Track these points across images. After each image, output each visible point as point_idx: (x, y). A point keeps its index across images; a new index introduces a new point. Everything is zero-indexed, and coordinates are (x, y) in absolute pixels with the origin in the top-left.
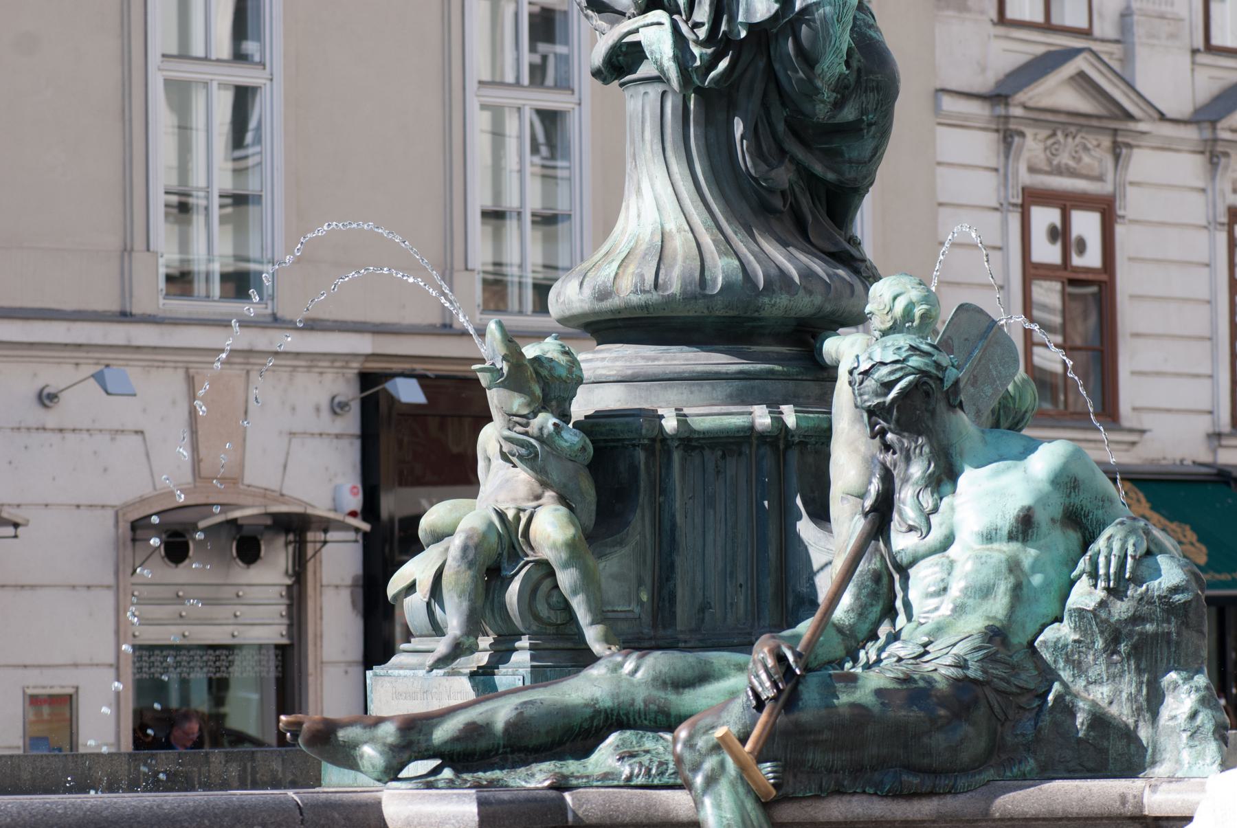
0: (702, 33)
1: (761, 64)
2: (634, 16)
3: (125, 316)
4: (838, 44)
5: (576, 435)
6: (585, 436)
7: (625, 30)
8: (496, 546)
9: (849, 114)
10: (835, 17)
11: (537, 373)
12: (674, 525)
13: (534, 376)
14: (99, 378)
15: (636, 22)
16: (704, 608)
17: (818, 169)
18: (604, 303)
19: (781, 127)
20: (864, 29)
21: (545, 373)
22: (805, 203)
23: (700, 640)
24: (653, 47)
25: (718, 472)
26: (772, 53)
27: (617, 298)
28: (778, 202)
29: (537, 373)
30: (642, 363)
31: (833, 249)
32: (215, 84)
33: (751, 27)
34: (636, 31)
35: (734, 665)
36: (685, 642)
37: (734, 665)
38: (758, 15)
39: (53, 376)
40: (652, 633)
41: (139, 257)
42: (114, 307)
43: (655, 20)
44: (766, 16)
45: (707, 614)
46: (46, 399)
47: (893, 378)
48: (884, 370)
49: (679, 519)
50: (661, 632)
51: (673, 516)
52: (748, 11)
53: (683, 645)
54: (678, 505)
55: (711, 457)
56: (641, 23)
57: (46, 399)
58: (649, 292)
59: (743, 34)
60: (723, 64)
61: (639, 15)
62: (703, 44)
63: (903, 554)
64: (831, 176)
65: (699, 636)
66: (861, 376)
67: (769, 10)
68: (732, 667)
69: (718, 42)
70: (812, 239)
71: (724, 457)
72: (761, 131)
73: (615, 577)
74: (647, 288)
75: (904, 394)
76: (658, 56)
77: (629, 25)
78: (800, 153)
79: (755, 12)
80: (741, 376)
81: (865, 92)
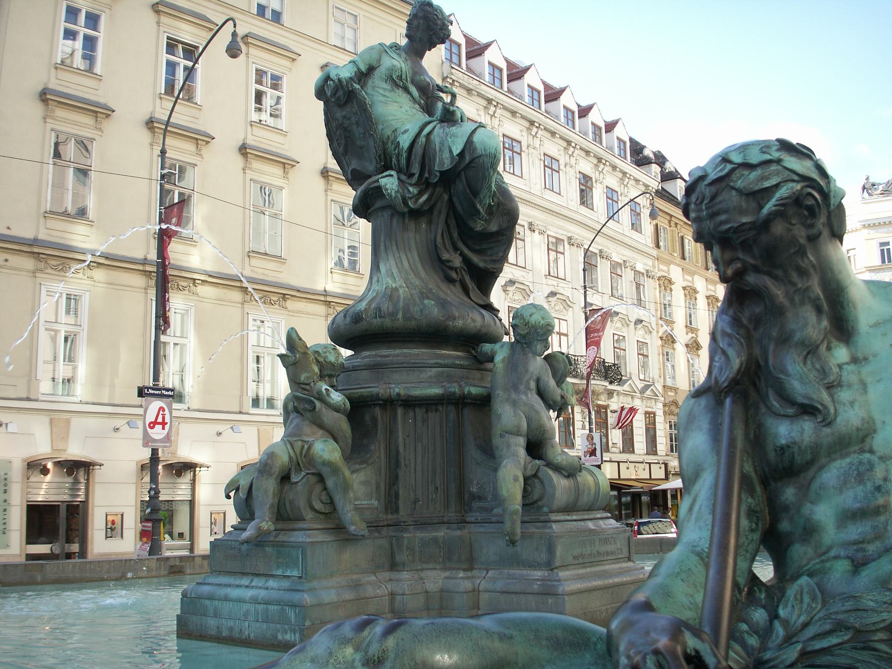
0: (414, 180)
1: (446, 197)
3: (241, 413)
4: (489, 183)
5: (339, 396)
6: (345, 398)
8: (287, 464)
9: (493, 228)
10: (489, 165)
11: (317, 360)
12: (398, 452)
13: (315, 361)
14: (232, 428)
16: (415, 502)
17: (475, 259)
18: (358, 325)
19: (455, 235)
20: (500, 183)
21: (321, 359)
22: (467, 279)
23: (414, 521)
25: (424, 421)
26: (452, 191)
27: (365, 321)
28: (454, 275)
29: (317, 360)
30: (379, 359)
31: (482, 303)
32: (266, 353)
33: (442, 172)
35: (547, 639)
36: (405, 522)
37: (547, 639)
39: (220, 427)
40: (385, 517)
41: (245, 397)
42: (238, 410)
45: (417, 505)
46: (219, 434)
47: (767, 184)
48: (754, 175)
49: (401, 449)
50: (390, 516)
51: (398, 447)
52: (442, 163)
53: (404, 524)
54: (400, 439)
55: (419, 412)
57: (219, 434)
58: (384, 317)
60: (425, 197)
63: (796, 450)
64: (481, 265)
65: (412, 519)
66: (713, 189)
68: (544, 642)
69: (424, 184)
70: (473, 299)
71: (427, 411)
72: (445, 236)
73: (362, 483)
74: (383, 315)
75: (784, 204)
76: (389, 191)
78: (466, 251)
79: (444, 164)
80: (437, 366)
81: (502, 216)
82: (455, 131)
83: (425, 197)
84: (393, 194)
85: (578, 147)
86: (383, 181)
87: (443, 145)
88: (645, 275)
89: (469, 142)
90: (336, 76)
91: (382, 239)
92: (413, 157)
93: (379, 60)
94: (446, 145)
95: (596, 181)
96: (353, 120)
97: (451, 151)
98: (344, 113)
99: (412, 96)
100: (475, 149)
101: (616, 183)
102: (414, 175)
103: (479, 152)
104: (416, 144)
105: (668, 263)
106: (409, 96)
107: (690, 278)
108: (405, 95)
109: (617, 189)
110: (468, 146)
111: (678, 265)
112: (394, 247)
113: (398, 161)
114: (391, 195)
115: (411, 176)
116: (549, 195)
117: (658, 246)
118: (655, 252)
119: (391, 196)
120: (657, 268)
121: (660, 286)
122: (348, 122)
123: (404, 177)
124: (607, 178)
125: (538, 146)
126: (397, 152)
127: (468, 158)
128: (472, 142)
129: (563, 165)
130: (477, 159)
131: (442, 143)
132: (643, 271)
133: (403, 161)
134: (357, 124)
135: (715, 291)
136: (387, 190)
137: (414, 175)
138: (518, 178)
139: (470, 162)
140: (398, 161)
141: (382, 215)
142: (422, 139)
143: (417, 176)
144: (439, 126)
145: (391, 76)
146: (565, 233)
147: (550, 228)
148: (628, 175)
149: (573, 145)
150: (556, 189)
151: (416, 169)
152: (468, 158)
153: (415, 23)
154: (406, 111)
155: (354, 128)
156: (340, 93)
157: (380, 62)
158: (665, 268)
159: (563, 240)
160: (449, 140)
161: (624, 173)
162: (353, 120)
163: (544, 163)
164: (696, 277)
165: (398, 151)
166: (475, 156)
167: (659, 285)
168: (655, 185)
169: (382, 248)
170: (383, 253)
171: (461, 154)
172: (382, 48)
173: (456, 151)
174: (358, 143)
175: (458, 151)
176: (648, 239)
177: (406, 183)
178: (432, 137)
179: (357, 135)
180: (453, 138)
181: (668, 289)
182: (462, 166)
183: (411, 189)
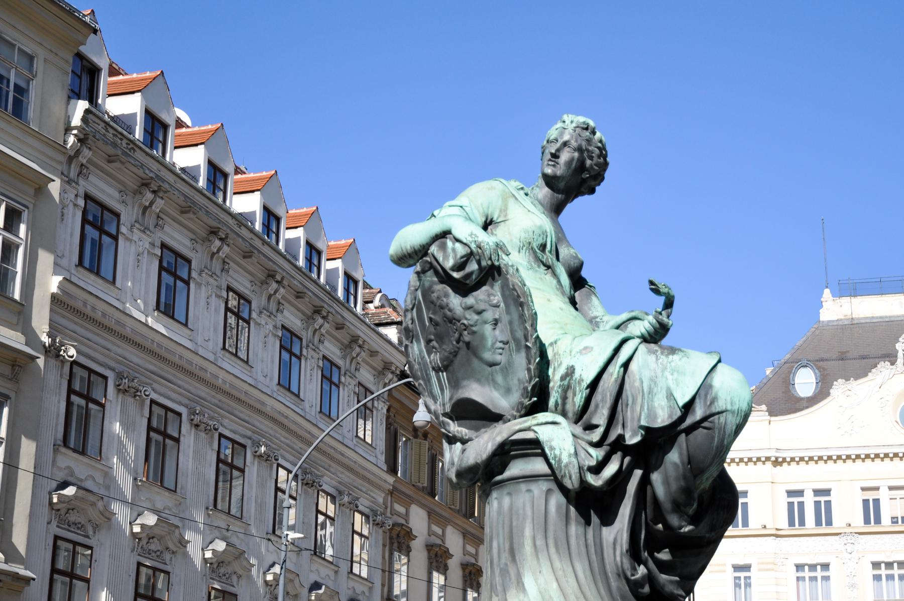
0: (596, 436)
1: (638, 473)
2: (515, 418)
7: (517, 428)
15: (525, 422)
24: (554, 444)
33: (648, 430)
34: (528, 429)
38: (659, 420)
43: (550, 419)
44: (667, 422)
52: (652, 415)
56: (535, 422)
59: (633, 439)
61: (521, 416)
62: (597, 445)
67: (670, 416)
76: (557, 452)
77: (521, 423)
82: (679, 363)
83: (611, 469)
84: (565, 459)
85: (285, 283)
86: (545, 434)
87: (655, 383)
88: (371, 519)
89: (705, 387)
90: (471, 235)
91: (528, 532)
92: (597, 397)
93: (504, 210)
94: (662, 384)
95: (308, 346)
96: (489, 315)
97: (670, 396)
98: (470, 300)
99: (559, 282)
100: (714, 400)
101: (338, 352)
102: (596, 426)
103: (720, 405)
104: (605, 376)
105: (407, 501)
106: (555, 282)
107: (439, 531)
108: (549, 277)
109: (340, 362)
110: (702, 392)
111: (422, 506)
112: (552, 550)
113: (564, 398)
114: (560, 460)
115: (590, 427)
116: (229, 363)
117: (393, 470)
118: (391, 479)
119: (560, 461)
120: (389, 510)
121: (392, 543)
122: (476, 317)
123: (578, 429)
124: (326, 343)
125: (218, 272)
126: (566, 383)
127: (699, 413)
128: (711, 386)
129: (257, 310)
130: (717, 417)
131: (653, 381)
132: (367, 511)
133: (578, 399)
134: (496, 322)
135: (476, 556)
136: (552, 448)
137: (596, 426)
138: (179, 325)
139: (705, 419)
140: (564, 398)
141: (529, 491)
142: (615, 370)
143: (601, 430)
144: (643, 348)
145: (530, 243)
146: (249, 433)
147: (226, 422)
148: (360, 342)
149: (278, 278)
150: (242, 354)
151: (600, 418)
152: (699, 413)
153: (565, 156)
154: (561, 309)
155: (488, 328)
156: (473, 266)
157: (506, 215)
158: (401, 510)
159: (244, 447)
160: (670, 377)
161: (355, 339)
162: (489, 315)
163: (226, 303)
164: (450, 530)
165: (569, 382)
166: (715, 409)
167: (391, 538)
168: (400, 361)
169: (528, 548)
170: (529, 558)
171: (688, 407)
172: (507, 190)
173: (683, 399)
174: (488, 356)
175: (687, 398)
176: (379, 456)
177: (583, 439)
178: (633, 366)
179: (489, 343)
180: (675, 374)
181: (404, 547)
182: (689, 421)
183: (592, 451)
